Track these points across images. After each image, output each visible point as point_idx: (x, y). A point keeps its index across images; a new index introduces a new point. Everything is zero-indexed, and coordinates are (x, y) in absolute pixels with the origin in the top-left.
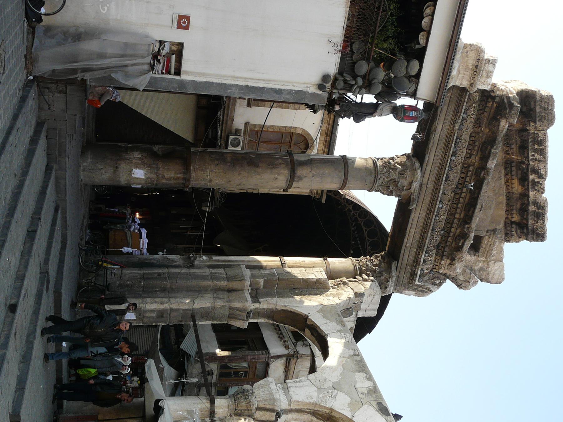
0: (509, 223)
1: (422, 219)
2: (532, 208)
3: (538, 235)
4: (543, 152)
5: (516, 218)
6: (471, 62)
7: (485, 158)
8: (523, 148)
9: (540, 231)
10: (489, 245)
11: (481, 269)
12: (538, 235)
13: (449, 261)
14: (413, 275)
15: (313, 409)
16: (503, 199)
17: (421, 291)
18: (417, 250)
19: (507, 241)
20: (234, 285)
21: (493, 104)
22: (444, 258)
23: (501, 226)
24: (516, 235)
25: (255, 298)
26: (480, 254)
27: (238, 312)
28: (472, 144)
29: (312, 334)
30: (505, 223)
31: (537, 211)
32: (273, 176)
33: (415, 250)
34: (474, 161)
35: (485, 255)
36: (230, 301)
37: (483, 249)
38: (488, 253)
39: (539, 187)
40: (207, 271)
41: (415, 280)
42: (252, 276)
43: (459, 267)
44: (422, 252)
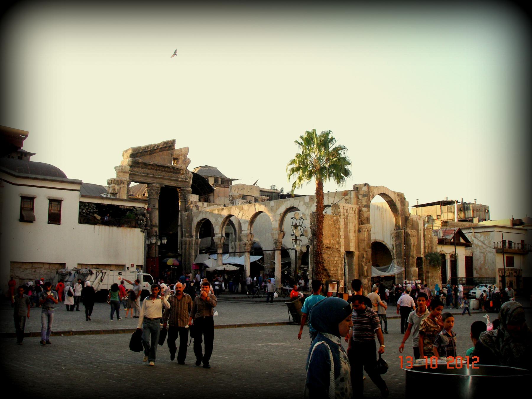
0: (169, 150)
1: (167, 181)
2: (165, 146)
4: (148, 147)
6: (122, 174)
7: (150, 165)
8: (146, 152)
11: (184, 156)
12: (173, 142)
14: (185, 181)
16: (161, 153)
20: (188, 243)
21: (134, 164)
23: (169, 152)
25: (192, 237)
28: (144, 168)
38: (178, 155)
39: (158, 146)
40: (183, 251)
42: (185, 237)
43: (183, 167)
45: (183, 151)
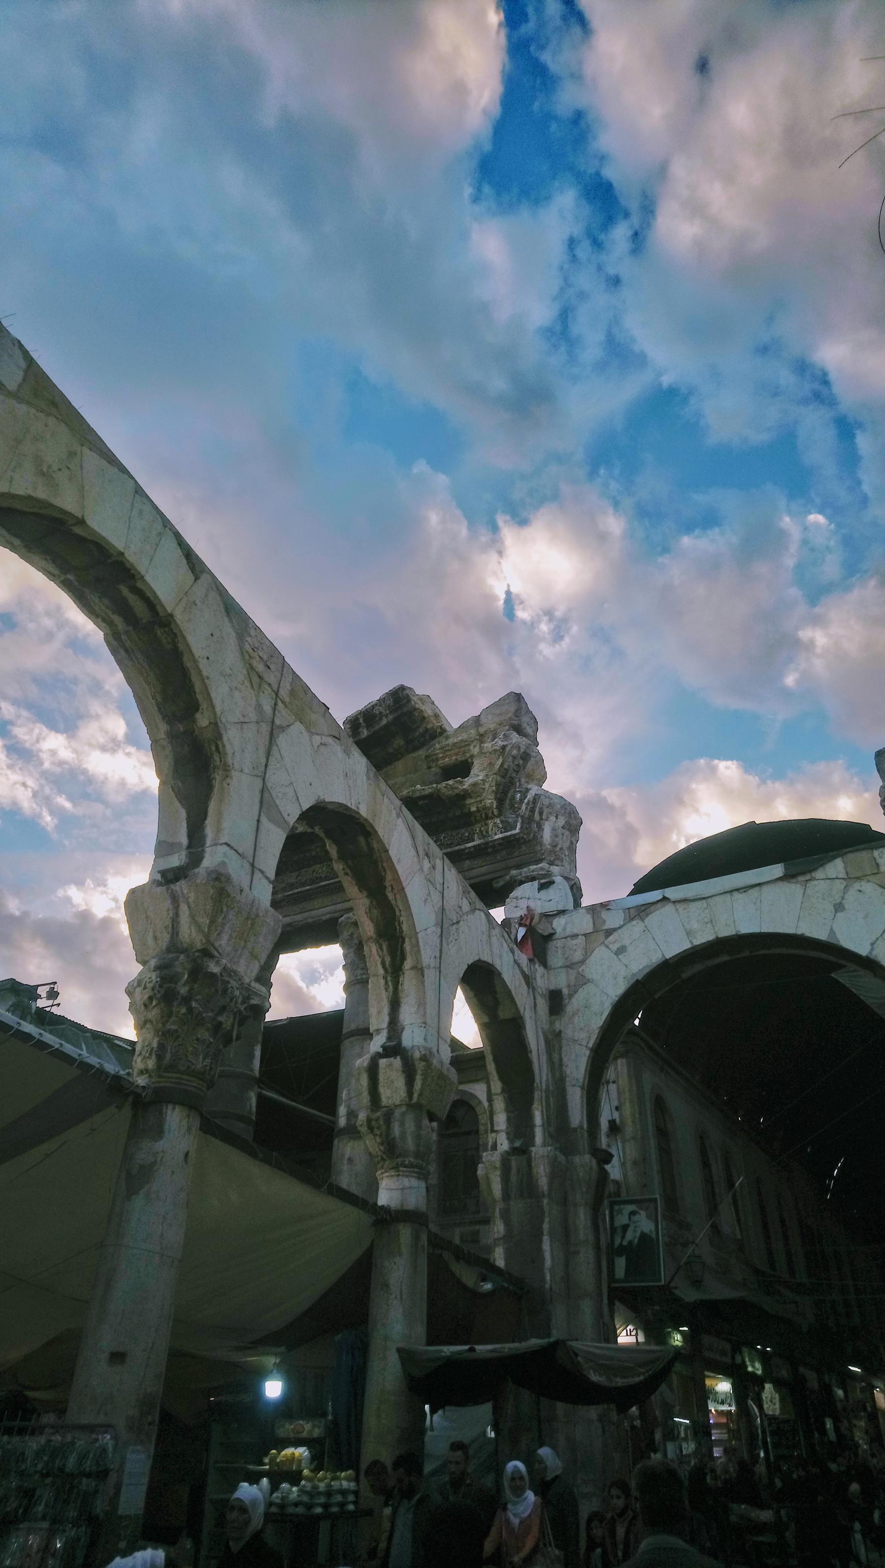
0: (413, 745)
3: (400, 697)
5: (399, 742)
9: (390, 702)
10: (448, 753)
12: (400, 697)
13: (469, 801)
15: (385, 978)
17: (541, 813)
18: (466, 859)
19: (443, 731)
22: (466, 811)
24: (424, 725)
26: (468, 755)
27: (514, 1178)
29: (497, 1003)
30: (416, 749)
31: (363, 724)
32: (345, 1167)
33: (467, 862)
34: (318, 850)
35: (467, 748)
36: (494, 1201)
37: (458, 757)
41: (514, 835)
44: (462, 850)
45: (483, 720)
